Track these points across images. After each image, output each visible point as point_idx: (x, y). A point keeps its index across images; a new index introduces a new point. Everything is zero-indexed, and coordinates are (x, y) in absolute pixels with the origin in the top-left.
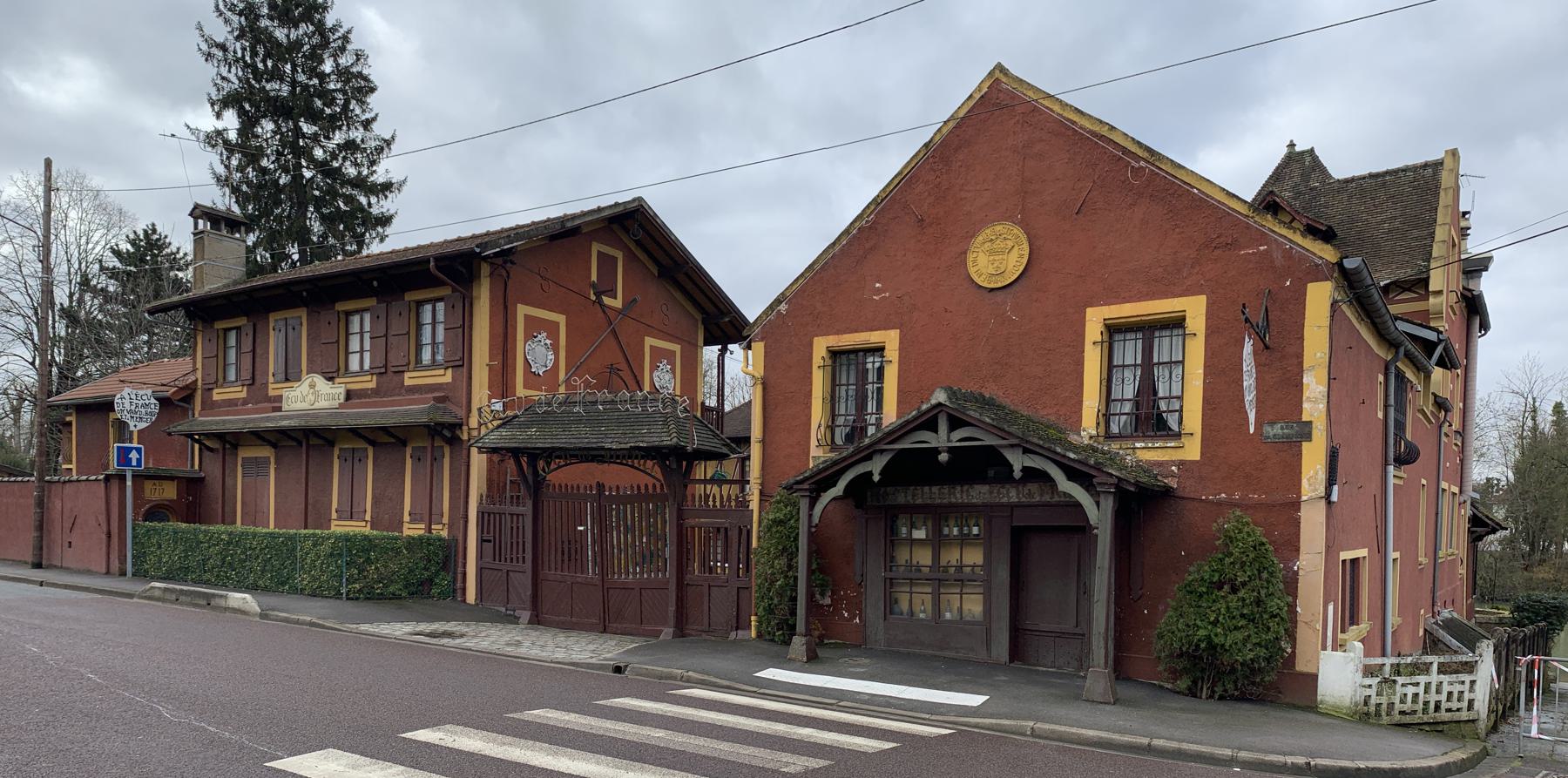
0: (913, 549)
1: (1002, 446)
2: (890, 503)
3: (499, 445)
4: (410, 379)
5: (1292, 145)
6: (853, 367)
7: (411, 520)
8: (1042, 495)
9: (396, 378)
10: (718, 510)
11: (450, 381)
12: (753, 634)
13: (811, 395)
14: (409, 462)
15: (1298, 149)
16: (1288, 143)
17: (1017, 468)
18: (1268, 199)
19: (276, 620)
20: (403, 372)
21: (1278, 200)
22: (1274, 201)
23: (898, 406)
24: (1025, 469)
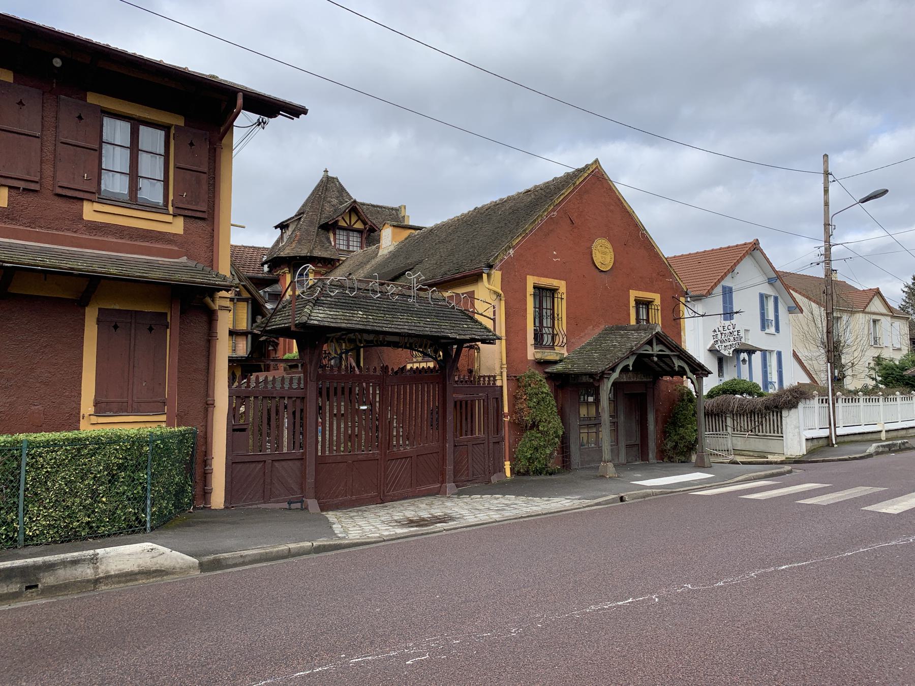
0: (589, 408)
1: (672, 355)
3: (339, 325)
4: (90, 212)
5: (326, 171)
6: (548, 298)
7: (96, 412)
8: (633, 378)
9: (63, 205)
10: (486, 387)
11: (181, 232)
12: (508, 474)
14: (91, 333)
16: (324, 170)
17: (676, 366)
19: (244, 564)
20: (82, 200)
21: (358, 207)
22: (356, 206)
24: (679, 366)
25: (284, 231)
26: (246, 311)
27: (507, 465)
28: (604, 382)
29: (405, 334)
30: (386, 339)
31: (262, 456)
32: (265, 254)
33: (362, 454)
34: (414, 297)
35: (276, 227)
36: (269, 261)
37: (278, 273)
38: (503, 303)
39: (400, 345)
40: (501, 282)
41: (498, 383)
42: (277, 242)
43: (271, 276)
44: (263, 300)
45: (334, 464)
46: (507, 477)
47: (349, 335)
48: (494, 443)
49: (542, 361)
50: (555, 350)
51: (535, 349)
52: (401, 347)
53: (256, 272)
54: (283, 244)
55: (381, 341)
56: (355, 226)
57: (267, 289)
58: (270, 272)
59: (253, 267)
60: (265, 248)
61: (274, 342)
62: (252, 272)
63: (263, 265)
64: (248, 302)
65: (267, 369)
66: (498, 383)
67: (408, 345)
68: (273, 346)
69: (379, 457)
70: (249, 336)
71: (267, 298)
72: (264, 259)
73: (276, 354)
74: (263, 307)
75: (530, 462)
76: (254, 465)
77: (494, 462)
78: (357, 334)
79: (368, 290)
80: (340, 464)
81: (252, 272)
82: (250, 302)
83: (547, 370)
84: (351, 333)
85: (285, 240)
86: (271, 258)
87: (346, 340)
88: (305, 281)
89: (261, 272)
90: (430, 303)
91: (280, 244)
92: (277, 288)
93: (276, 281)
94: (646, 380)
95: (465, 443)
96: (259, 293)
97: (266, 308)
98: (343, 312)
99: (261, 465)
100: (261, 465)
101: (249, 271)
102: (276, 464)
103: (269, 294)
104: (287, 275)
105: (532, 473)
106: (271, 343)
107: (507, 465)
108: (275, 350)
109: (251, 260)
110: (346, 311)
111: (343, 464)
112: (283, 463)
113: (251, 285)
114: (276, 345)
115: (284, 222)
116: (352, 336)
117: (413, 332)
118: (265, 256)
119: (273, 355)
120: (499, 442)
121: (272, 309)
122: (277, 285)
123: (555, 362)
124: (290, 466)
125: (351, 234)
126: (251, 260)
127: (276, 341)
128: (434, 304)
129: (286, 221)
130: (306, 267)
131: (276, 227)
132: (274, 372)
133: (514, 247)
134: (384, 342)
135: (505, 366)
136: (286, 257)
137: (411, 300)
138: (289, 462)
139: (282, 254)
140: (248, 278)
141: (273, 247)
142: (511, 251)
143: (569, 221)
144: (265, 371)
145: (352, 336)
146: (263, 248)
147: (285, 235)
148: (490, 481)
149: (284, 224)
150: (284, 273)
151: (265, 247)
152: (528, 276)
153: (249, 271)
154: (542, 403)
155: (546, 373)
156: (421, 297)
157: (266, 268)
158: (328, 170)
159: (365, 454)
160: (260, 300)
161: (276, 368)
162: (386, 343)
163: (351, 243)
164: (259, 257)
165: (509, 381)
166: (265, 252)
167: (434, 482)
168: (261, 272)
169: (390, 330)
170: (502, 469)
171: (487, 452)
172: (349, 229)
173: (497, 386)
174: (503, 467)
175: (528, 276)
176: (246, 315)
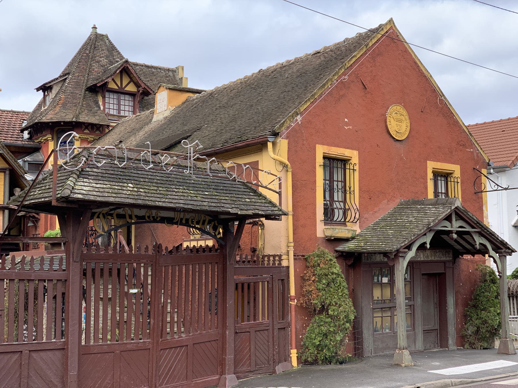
0: (383, 291)
2: (373, 261)
3: (106, 199)
5: (95, 28)
6: (339, 170)
10: (271, 267)
12: (295, 362)
13: (316, 184)
15: (99, 31)
16: (92, 26)
17: (478, 243)
18: (124, 65)
21: (130, 68)
22: (127, 67)
23: (359, 199)
24: (480, 244)
25: (46, 94)
26: (2, 183)
27: (294, 354)
28: (399, 260)
29: (180, 210)
30: (159, 215)
31: (18, 347)
32: (26, 119)
33: (132, 343)
34: (190, 167)
35: (38, 90)
36: (30, 127)
37: (39, 140)
38: (290, 175)
39: (174, 221)
40: (288, 151)
41: (284, 263)
42: (39, 106)
43: (32, 143)
44: (23, 171)
45: (100, 355)
46: (293, 366)
47: (117, 210)
48: (278, 329)
49: (333, 238)
50: (346, 226)
51: (325, 225)
52: (176, 223)
53: (15, 139)
54: (45, 108)
55: (153, 217)
56: (127, 89)
57: (27, 158)
58: (30, 139)
59: (11, 133)
60: (25, 113)
61: (34, 217)
62: (10, 139)
63: (22, 131)
64: (5, 172)
65: (26, 247)
66: (284, 263)
67: (184, 222)
68: (33, 222)
69: (150, 346)
70: (7, 212)
71: (27, 168)
72: (24, 125)
73: (36, 232)
74: (22, 179)
75: (318, 350)
76: (9, 355)
77: (279, 351)
78: (127, 209)
79: (140, 160)
80: (106, 354)
81: (10, 139)
82: (7, 172)
83: (338, 249)
84: (120, 208)
85: (48, 103)
86: (31, 124)
87: (115, 216)
88: (68, 151)
89: (21, 139)
90: (208, 175)
91: (43, 108)
92: (38, 157)
93: (36, 150)
94: (444, 259)
95: (248, 330)
96: (18, 163)
97: (26, 179)
98: (111, 185)
99: (16, 356)
100: (18, 355)
101: (6, 138)
102: (34, 355)
103: (28, 163)
104: (49, 142)
105: (320, 362)
106: (31, 219)
107: (294, 354)
108: (36, 227)
109: (9, 126)
110: (114, 183)
111: (110, 354)
112: (42, 354)
113: (8, 153)
114: (36, 221)
115: (46, 84)
116: (120, 211)
117: (190, 207)
118: (25, 122)
119: (32, 232)
120: (285, 328)
121: (32, 180)
122: (38, 154)
123: (347, 240)
124: (50, 357)
125: (122, 97)
126: (9, 126)
127: (36, 216)
128: (213, 176)
129: (50, 82)
130: (71, 133)
131: (38, 90)
132: (33, 251)
133: (301, 114)
134: (157, 218)
135: (292, 244)
136: (48, 123)
137: (187, 172)
138: (49, 353)
139: (44, 120)
140: (5, 146)
141: (34, 112)
142: (299, 118)
143: (362, 86)
144: (23, 251)
145: (120, 211)
146: (23, 112)
147: (47, 98)
148: (274, 372)
149: (47, 86)
150: (47, 140)
151: (26, 111)
152: (317, 146)
153: (6, 138)
154: (332, 285)
155: (337, 251)
156: (198, 168)
157: (26, 135)
158: (97, 26)
159: (134, 343)
160: (19, 171)
161: (36, 247)
162: (158, 219)
163: (122, 108)
164: (19, 122)
165: (297, 262)
166: (26, 117)
167: (213, 374)
168: (21, 139)
169: (164, 205)
170: (287, 358)
171: (271, 340)
172: (120, 92)
173: (283, 267)
174: (289, 355)
175: (317, 146)
176: (3, 187)
